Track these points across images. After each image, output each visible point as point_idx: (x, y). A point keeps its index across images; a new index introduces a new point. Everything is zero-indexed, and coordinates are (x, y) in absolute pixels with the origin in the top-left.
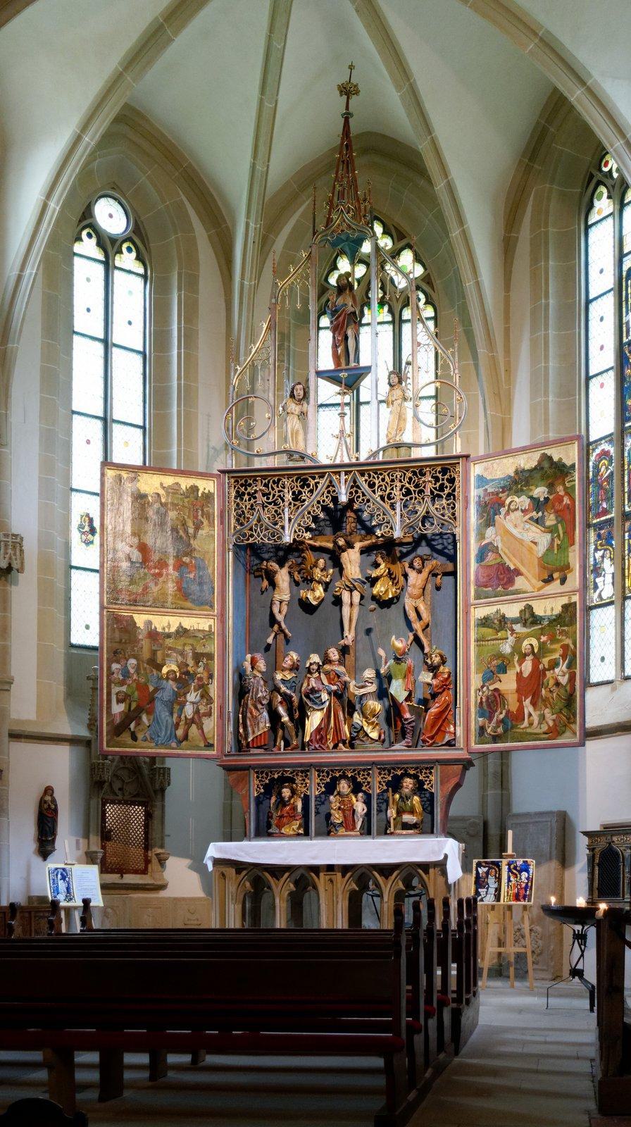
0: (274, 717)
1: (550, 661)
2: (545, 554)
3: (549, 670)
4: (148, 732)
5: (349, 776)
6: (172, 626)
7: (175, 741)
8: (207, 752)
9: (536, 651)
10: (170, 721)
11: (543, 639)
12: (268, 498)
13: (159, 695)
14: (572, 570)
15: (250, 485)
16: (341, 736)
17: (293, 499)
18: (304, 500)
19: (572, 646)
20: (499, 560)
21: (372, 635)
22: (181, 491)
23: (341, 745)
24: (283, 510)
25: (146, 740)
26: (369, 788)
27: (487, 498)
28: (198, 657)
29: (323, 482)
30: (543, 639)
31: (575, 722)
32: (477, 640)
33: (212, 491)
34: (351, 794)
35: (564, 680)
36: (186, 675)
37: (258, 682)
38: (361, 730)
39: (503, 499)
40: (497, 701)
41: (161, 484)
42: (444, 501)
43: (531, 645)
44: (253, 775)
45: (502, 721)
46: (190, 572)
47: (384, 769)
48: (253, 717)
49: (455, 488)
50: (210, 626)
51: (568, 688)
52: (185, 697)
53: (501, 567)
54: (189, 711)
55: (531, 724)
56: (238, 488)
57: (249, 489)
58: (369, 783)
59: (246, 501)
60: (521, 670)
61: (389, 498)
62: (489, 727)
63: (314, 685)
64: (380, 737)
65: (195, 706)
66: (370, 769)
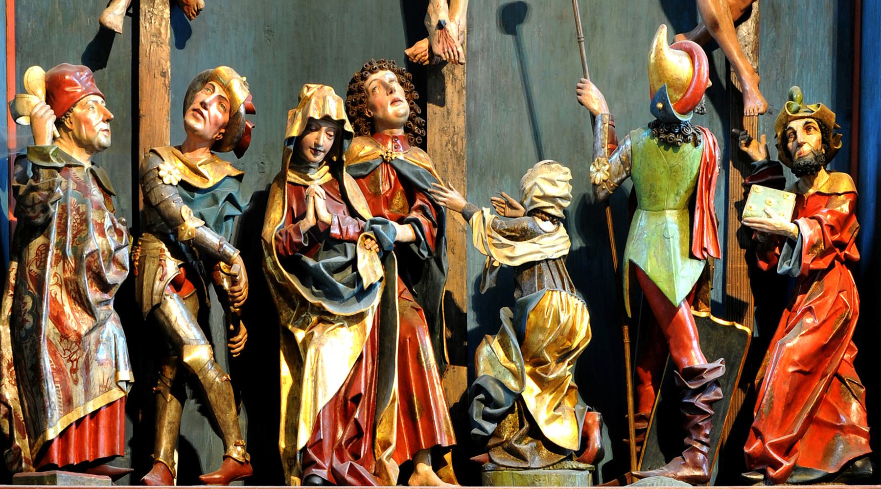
16: (434, 438)
23: (425, 468)
37: (83, 189)
38: (511, 410)
48: (64, 337)
63: (325, 216)
64: (585, 439)
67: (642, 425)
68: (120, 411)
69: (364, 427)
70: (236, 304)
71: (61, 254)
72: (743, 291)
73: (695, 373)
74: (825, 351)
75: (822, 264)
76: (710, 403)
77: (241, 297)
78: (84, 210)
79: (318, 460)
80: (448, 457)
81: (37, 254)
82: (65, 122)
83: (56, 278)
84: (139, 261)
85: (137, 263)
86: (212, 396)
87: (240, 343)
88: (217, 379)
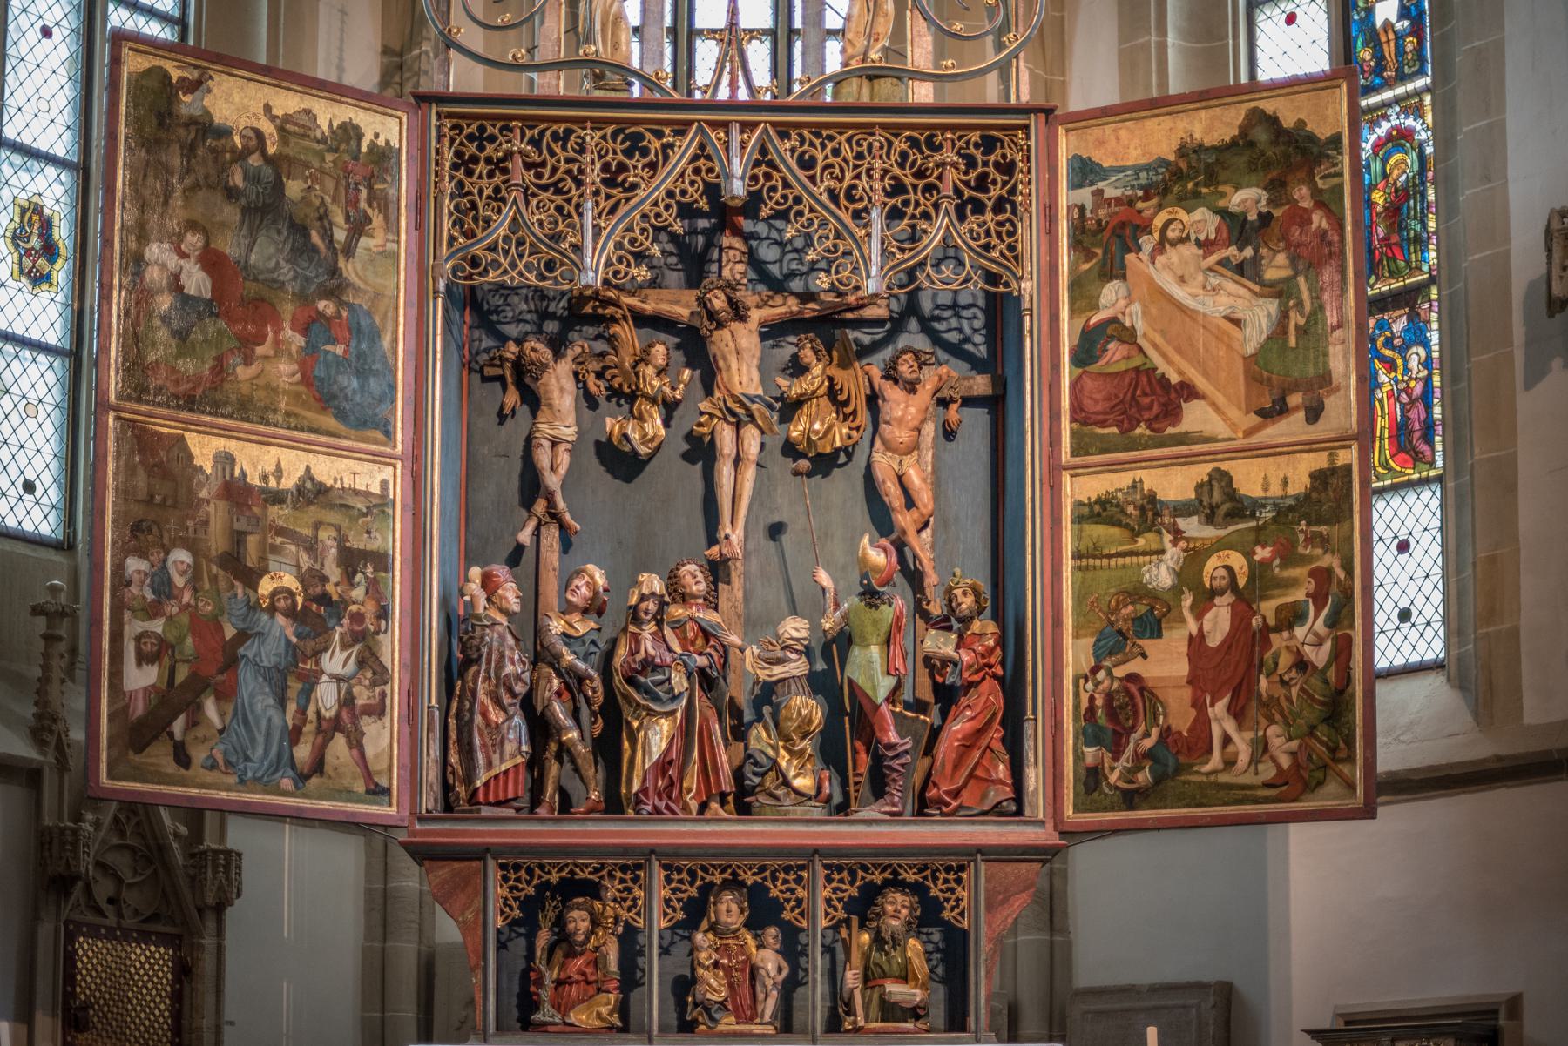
0: (540, 728)
1: (1279, 610)
2: (1263, 349)
3: (1278, 629)
4: (222, 747)
5: (749, 883)
6: (285, 474)
7: (291, 773)
8: (374, 809)
9: (1242, 582)
10: (277, 720)
11: (1262, 553)
12: (539, 176)
13: (248, 650)
14: (1338, 389)
15: (492, 139)
17: (604, 181)
18: (634, 186)
19: (1341, 574)
20: (1137, 361)
21: (786, 539)
22: (319, 135)
23: (715, 805)
24: (578, 206)
25: (213, 766)
26: (802, 914)
27: (1102, 213)
28: (351, 561)
29: (686, 147)
30: (1262, 553)
31: (1351, 759)
32: (1077, 555)
33: (395, 142)
34: (743, 930)
35: (1319, 656)
36: (320, 604)
38: (771, 769)
39: (1146, 214)
40: (1134, 706)
41: (268, 108)
42: (989, 216)
43: (1229, 569)
44: (494, 873)
45: (1150, 755)
46: (334, 341)
47: (840, 869)
49: (1014, 188)
50: (384, 484)
51: (1331, 674)
52: (318, 663)
53: (1144, 379)
54: (327, 697)
55: (1229, 763)
56: (461, 144)
57: (489, 149)
58: (799, 902)
59: (480, 177)
60: (1200, 629)
61: (850, 198)
62: (1112, 769)
63: (651, 651)
64: (819, 788)
65: (344, 686)
66: (802, 868)
67: (858, 779)
68: (522, 770)
69: (675, 779)
72: (927, 694)
73: (891, 747)
74: (980, 732)
75: (976, 678)
76: (903, 765)
80: (730, 798)
86: (579, 761)
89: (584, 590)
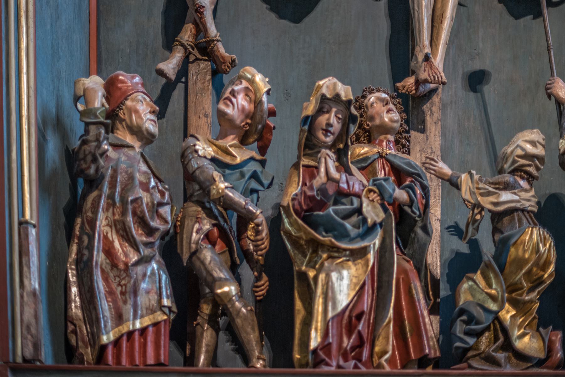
48: (114, 265)
70: (259, 253)
71: (111, 202)
77: (263, 246)
78: (131, 171)
79: (327, 359)
81: (92, 204)
82: (120, 114)
83: (107, 221)
84: (180, 221)
85: (179, 223)
87: (263, 287)
88: (244, 310)
89: (241, 101)
